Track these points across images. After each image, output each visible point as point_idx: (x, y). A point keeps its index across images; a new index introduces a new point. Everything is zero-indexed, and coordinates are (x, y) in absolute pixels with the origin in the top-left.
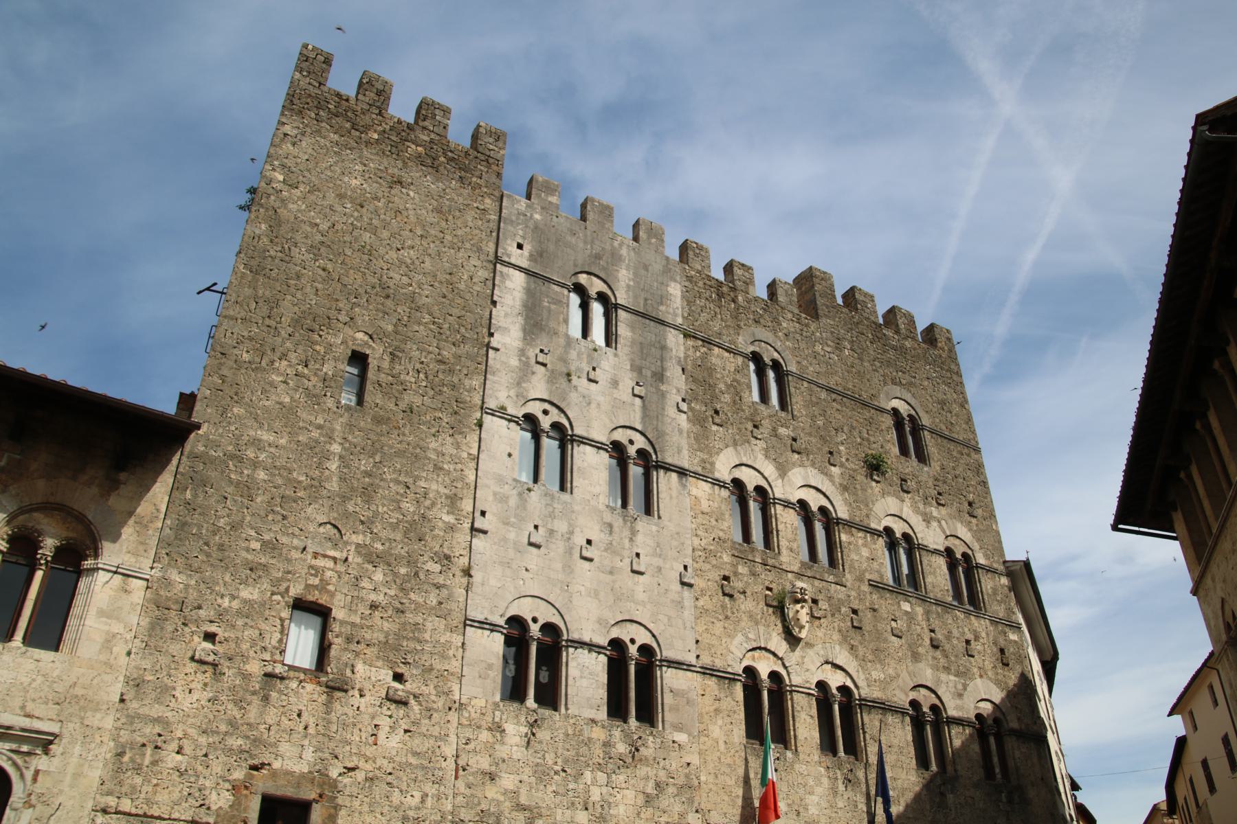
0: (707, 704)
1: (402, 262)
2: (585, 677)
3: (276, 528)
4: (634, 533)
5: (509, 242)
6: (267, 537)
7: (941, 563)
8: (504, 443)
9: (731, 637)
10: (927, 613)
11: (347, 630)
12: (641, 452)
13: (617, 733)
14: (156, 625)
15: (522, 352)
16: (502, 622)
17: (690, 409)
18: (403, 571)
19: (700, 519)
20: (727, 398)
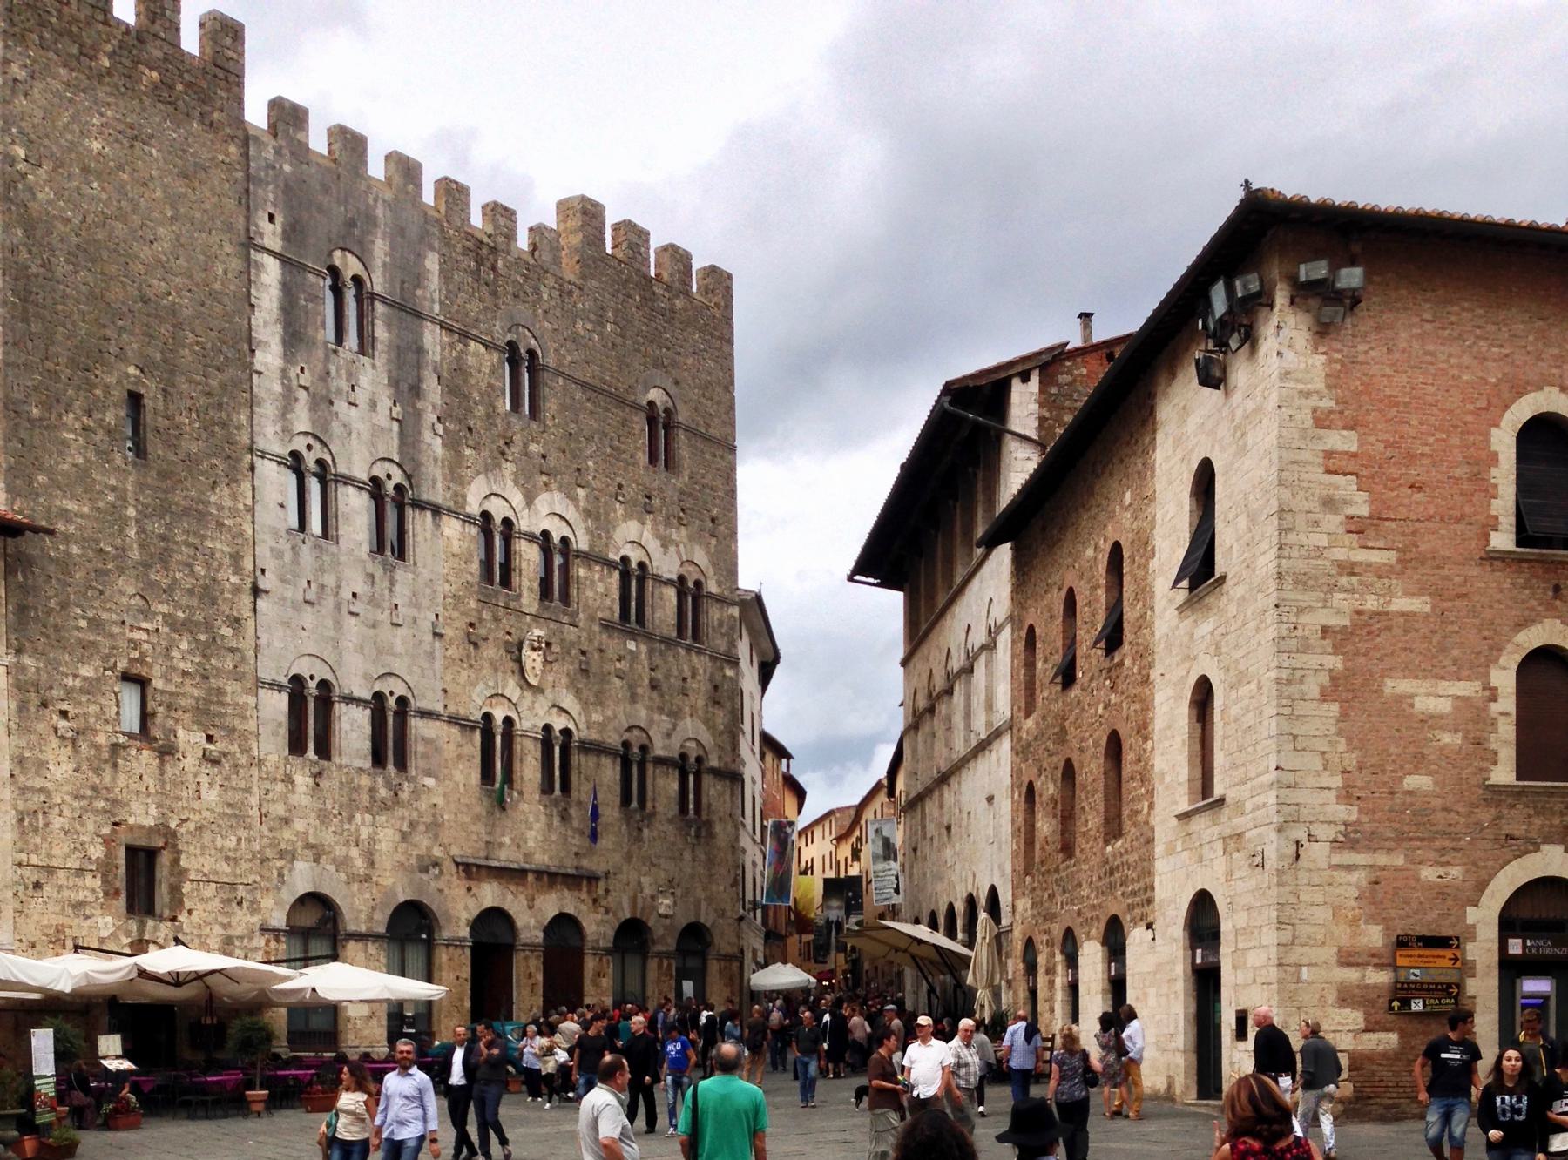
0: (450, 750)
1: (159, 261)
2: (353, 727)
3: (97, 604)
4: (392, 582)
5: (260, 213)
6: (90, 614)
7: (671, 594)
8: (275, 482)
9: (474, 685)
10: (651, 652)
11: (166, 698)
12: (398, 487)
13: (380, 780)
14: (22, 708)
15: (284, 373)
16: (285, 681)
17: (445, 429)
18: (203, 637)
19: (453, 562)
20: (480, 411)
